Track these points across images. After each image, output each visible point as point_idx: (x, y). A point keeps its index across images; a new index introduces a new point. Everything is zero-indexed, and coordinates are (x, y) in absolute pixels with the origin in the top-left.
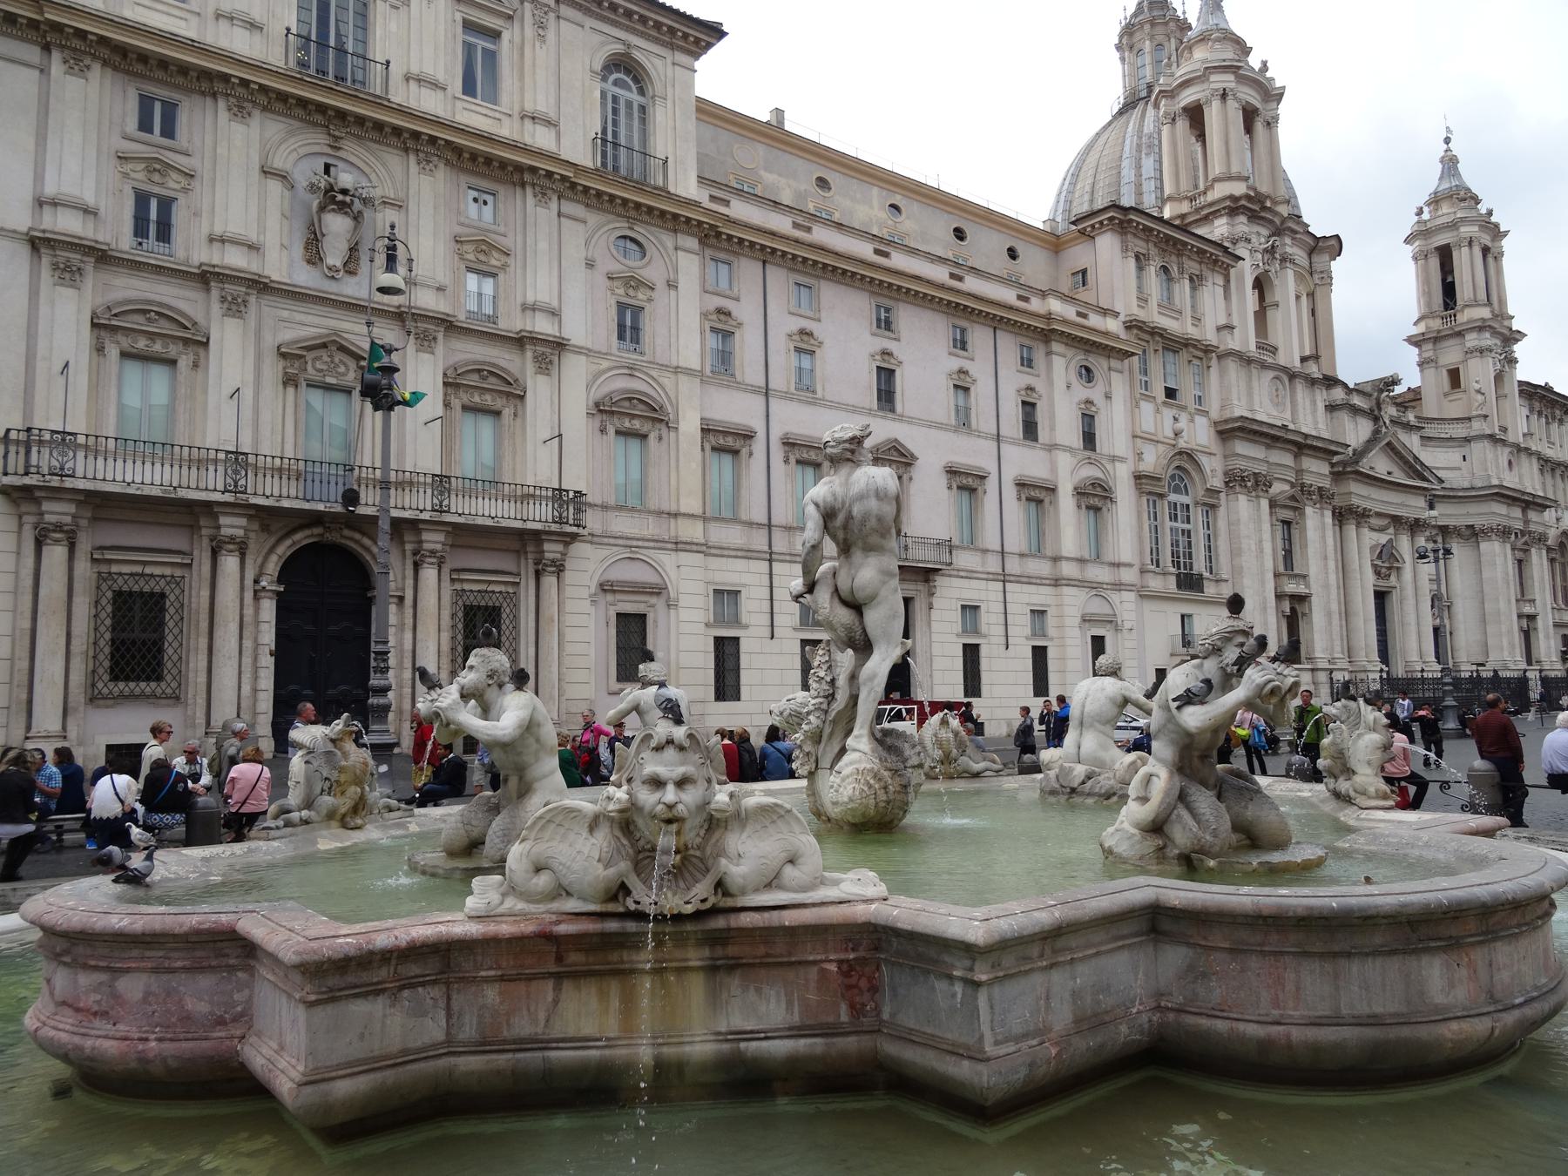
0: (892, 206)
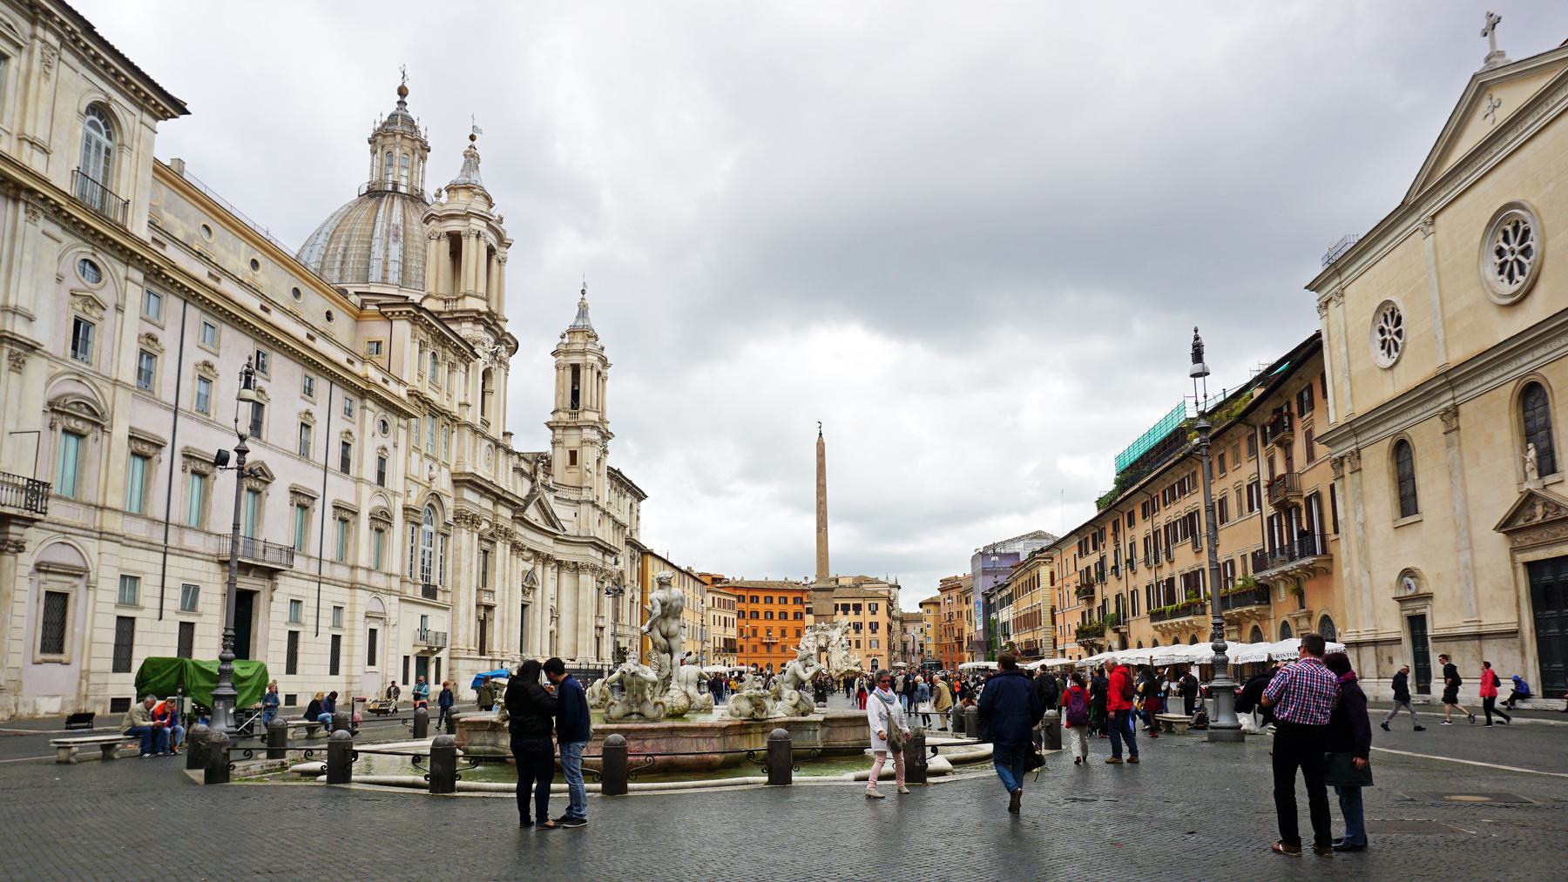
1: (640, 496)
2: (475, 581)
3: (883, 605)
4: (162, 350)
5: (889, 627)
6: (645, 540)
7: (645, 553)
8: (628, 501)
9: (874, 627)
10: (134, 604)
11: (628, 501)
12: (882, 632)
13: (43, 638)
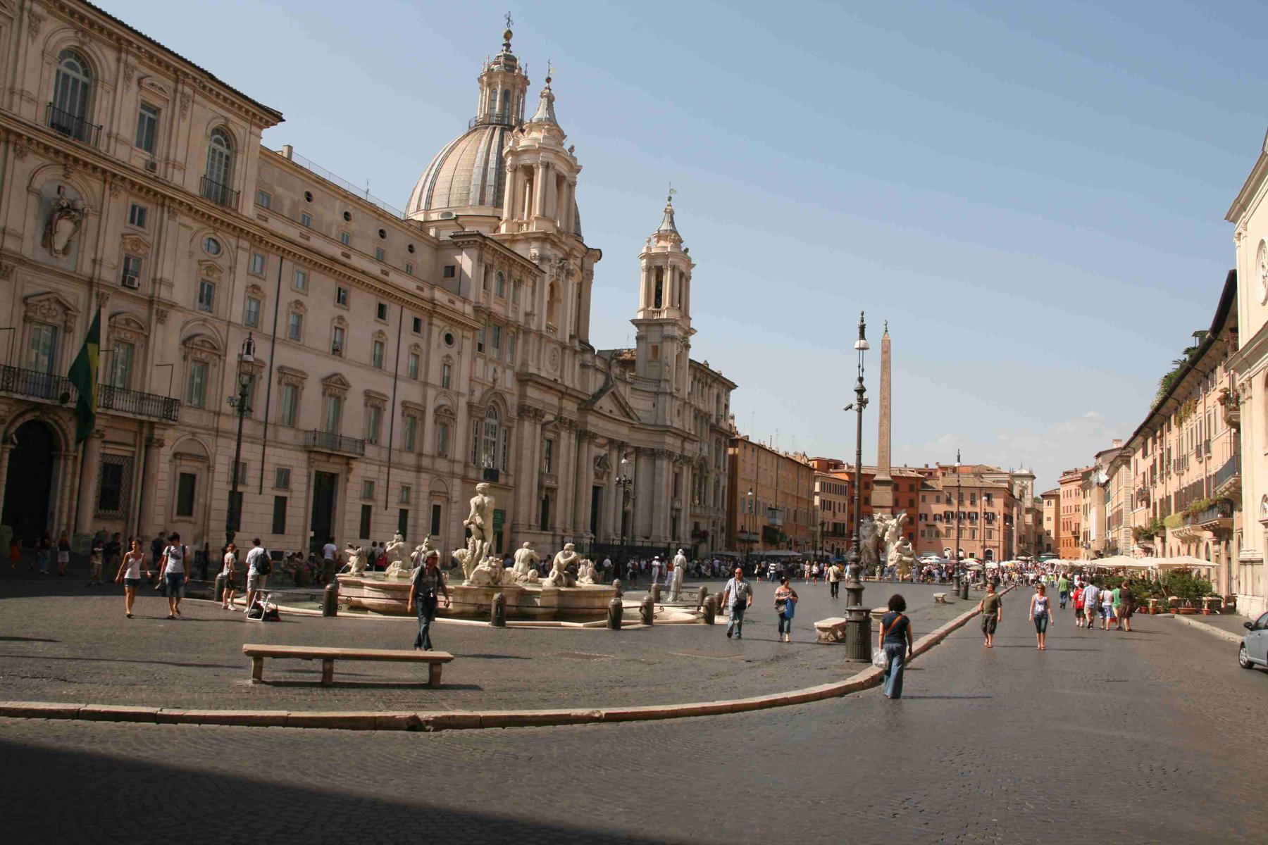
1: (731, 386)
7: (733, 439)
8: (715, 391)
9: (990, 518)
10: (407, 502)
11: (715, 391)
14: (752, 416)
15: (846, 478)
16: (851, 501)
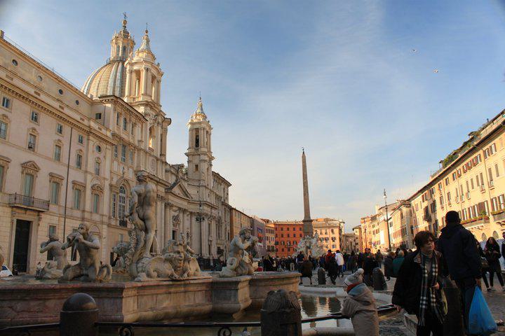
0: (14, 61)
1: (229, 185)
2: (207, 233)
3: (336, 231)
4: (38, 134)
5: (340, 239)
6: (232, 203)
7: (231, 209)
8: (223, 187)
9: (333, 239)
11: (223, 187)
12: (337, 242)
13: (14, 256)
14: (236, 199)
15: (273, 226)
16: (276, 236)
